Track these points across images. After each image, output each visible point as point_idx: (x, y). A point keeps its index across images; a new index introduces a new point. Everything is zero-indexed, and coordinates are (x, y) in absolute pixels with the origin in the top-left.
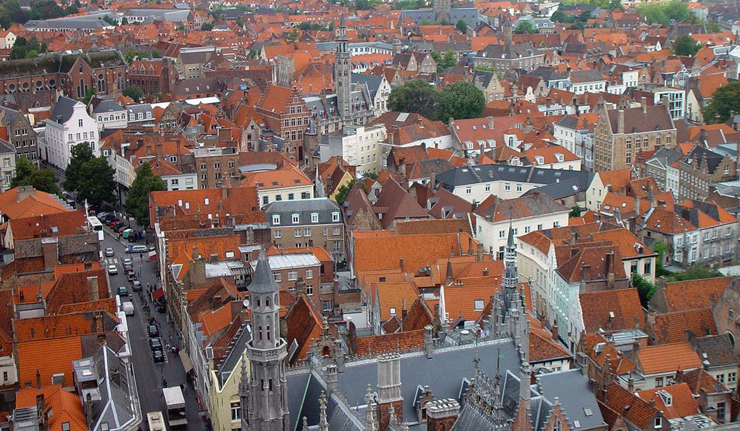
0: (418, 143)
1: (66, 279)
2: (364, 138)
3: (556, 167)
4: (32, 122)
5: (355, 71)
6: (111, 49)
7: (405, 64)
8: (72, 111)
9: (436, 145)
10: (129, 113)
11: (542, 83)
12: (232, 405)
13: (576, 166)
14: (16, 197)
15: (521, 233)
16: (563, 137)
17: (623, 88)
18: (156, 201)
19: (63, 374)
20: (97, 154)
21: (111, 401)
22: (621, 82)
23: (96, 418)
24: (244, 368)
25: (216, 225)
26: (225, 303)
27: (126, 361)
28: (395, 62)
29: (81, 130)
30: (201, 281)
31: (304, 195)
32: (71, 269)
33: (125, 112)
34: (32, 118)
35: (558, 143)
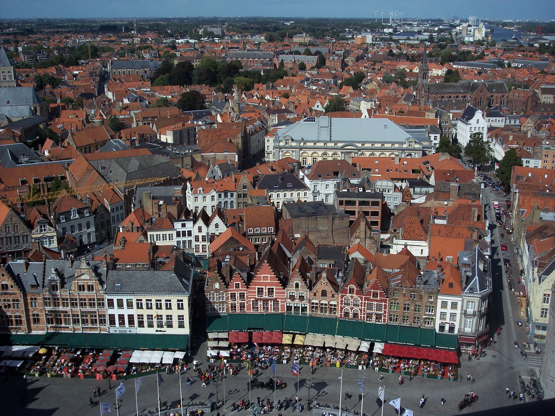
1: (460, 206)
6: (500, 82)
8: (474, 115)
10: (506, 119)
12: (545, 295)
14: (438, 158)
18: (516, 171)
19: (452, 257)
20: (485, 140)
21: (477, 277)
23: (467, 283)
25: (549, 191)
26: (549, 236)
27: (487, 257)
29: (477, 126)
32: (464, 202)
33: (504, 118)
34: (451, 115)
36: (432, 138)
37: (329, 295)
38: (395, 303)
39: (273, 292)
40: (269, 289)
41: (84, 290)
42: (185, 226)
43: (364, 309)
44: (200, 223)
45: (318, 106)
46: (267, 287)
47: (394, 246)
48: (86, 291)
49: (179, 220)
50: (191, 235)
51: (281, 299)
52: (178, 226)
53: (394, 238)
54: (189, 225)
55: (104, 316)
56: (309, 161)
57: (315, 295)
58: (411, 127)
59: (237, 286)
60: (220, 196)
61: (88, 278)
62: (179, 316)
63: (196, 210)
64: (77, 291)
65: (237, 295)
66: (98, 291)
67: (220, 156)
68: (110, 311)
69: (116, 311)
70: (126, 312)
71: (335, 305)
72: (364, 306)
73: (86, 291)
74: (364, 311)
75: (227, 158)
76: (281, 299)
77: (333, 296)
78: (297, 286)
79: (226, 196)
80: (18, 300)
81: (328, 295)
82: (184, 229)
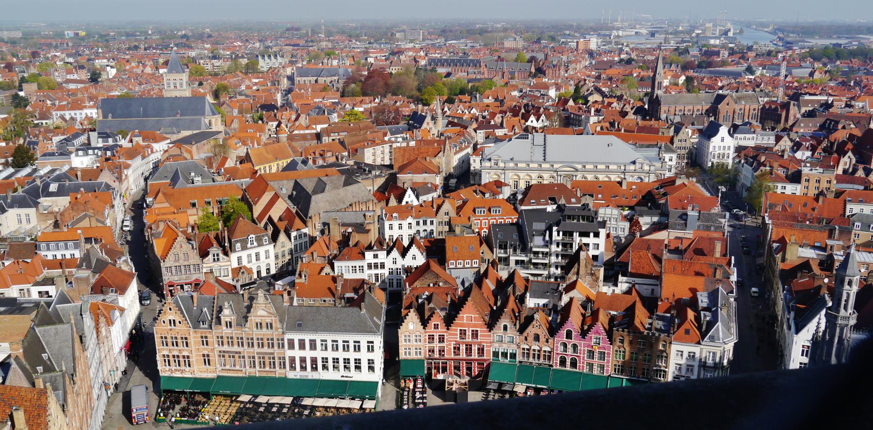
4: (690, 135)
12: (803, 346)
24: (819, 323)
25: (810, 222)
29: (722, 144)
30: (794, 258)
33: (755, 136)
36: (667, 159)
37: (542, 339)
38: (620, 351)
39: (477, 335)
40: (473, 331)
41: (261, 327)
42: (377, 257)
43: (584, 357)
44: (395, 253)
45: (532, 122)
46: (471, 329)
47: (619, 284)
48: (264, 329)
49: (370, 248)
50: (384, 268)
51: (486, 343)
52: (369, 255)
53: (620, 276)
54: (382, 254)
55: (284, 358)
56: (522, 186)
57: (526, 339)
58: (642, 146)
59: (436, 326)
60: (418, 223)
61: (264, 313)
62: (369, 360)
63: (389, 239)
64: (255, 329)
65: (436, 338)
66: (277, 329)
67: (419, 178)
68: (289, 353)
69: (297, 353)
70: (308, 354)
71: (550, 352)
72: (584, 354)
73: (264, 329)
74: (583, 359)
75: (427, 181)
76: (486, 343)
77: (547, 341)
78: (505, 328)
79: (425, 223)
80: (186, 338)
81: (541, 340)
82: (376, 261)
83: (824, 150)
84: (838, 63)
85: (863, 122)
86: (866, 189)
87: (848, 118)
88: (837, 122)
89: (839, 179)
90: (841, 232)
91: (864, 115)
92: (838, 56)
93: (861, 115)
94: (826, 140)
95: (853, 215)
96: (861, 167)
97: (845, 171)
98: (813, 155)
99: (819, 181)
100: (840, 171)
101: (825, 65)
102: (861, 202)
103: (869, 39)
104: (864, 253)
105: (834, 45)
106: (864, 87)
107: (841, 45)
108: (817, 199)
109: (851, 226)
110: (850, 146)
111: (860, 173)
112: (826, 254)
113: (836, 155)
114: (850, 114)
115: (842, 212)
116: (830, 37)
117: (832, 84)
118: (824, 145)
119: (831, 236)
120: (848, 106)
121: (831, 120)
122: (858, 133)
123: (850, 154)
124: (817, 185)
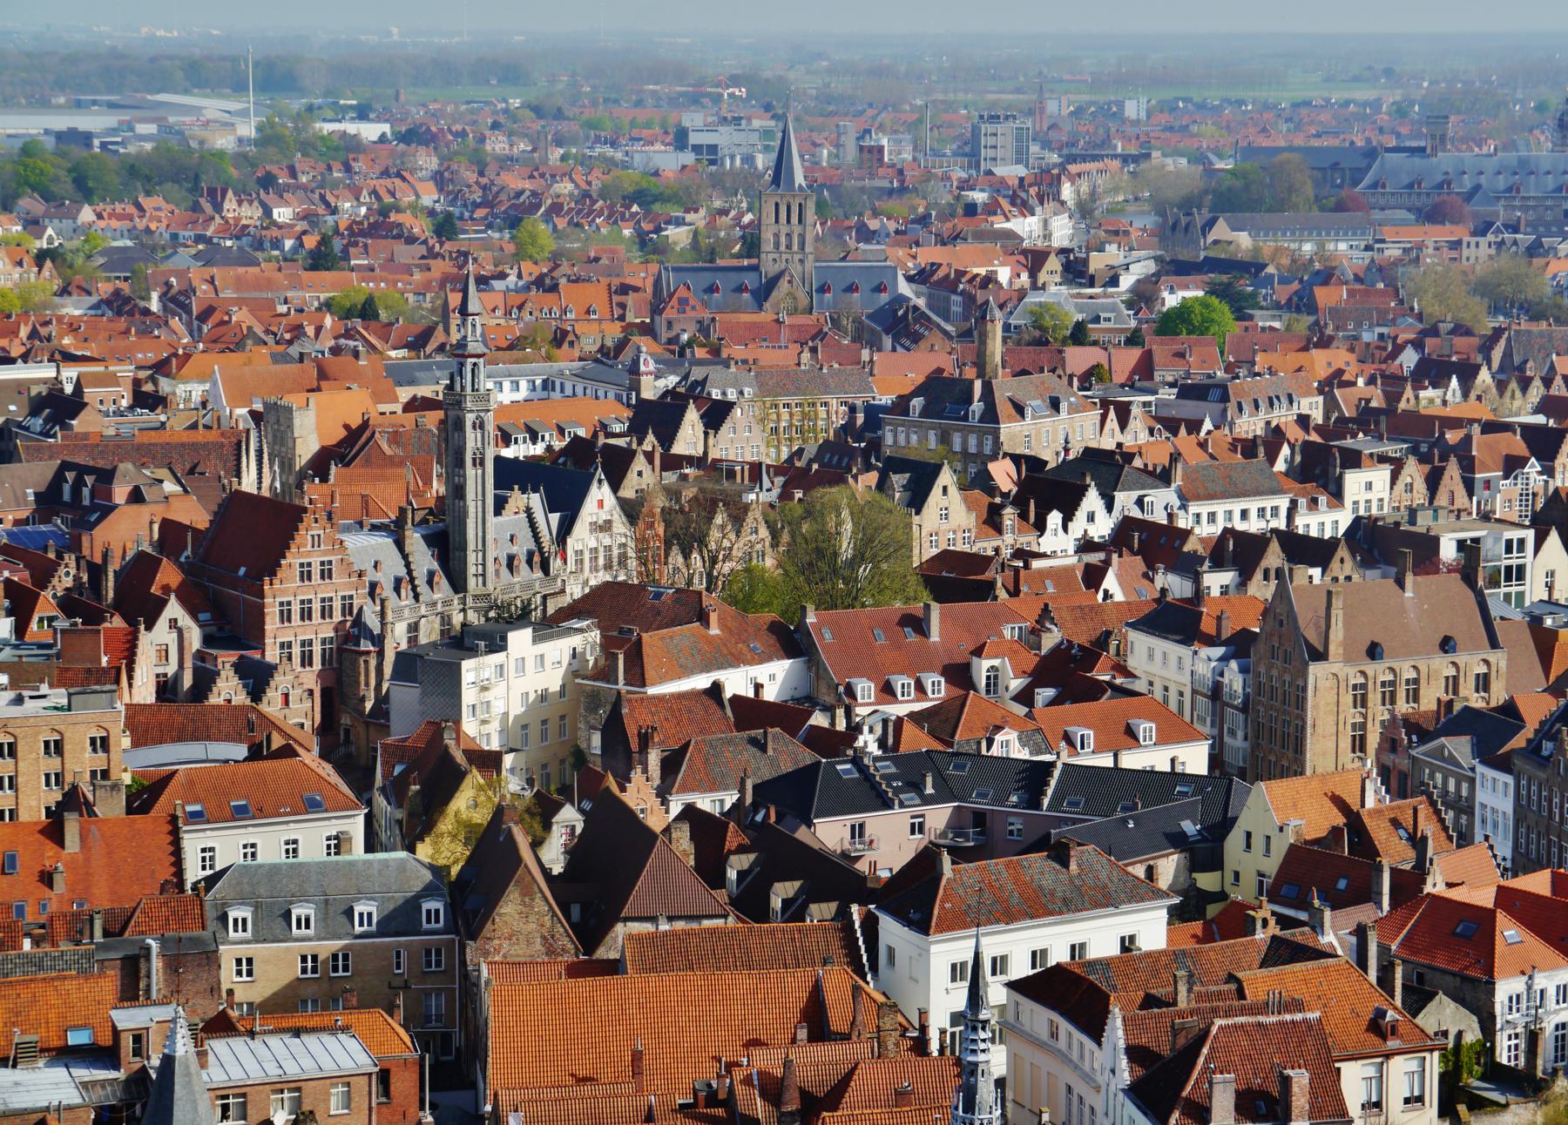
0: (702, 682)
2: (530, 664)
3: (1132, 760)
5: (508, 453)
7: (667, 438)
9: (758, 687)
11: (1092, 500)
13: (1195, 759)
15: (1021, 968)
16: (1156, 668)
17: (1344, 519)
22: (1337, 495)
25: (37, 942)
28: (637, 429)
31: (338, 843)
35: (1140, 686)
83: (68, 604)
84: (87, 214)
85: (210, 467)
86: (255, 754)
87: (144, 454)
88: (106, 477)
89: (144, 728)
90: (174, 965)
91: (212, 436)
92: (85, 189)
93: (200, 436)
94: (70, 559)
95: (211, 881)
96: (226, 659)
97: (166, 689)
98: (20, 629)
99: (56, 748)
100: (143, 690)
101: (33, 225)
102: (240, 814)
103: (188, 109)
104: (274, 1041)
105: (60, 136)
106: (205, 315)
107: (86, 138)
108: (53, 830)
109: (212, 925)
110: (169, 574)
111: (228, 689)
112: (120, 1075)
113: (117, 622)
114: (154, 437)
115: (166, 873)
116: (42, 104)
117: (73, 308)
118: (64, 580)
119: (132, 990)
120: (146, 400)
121: (82, 470)
122: (195, 514)
123: (173, 609)
124: (54, 764)
